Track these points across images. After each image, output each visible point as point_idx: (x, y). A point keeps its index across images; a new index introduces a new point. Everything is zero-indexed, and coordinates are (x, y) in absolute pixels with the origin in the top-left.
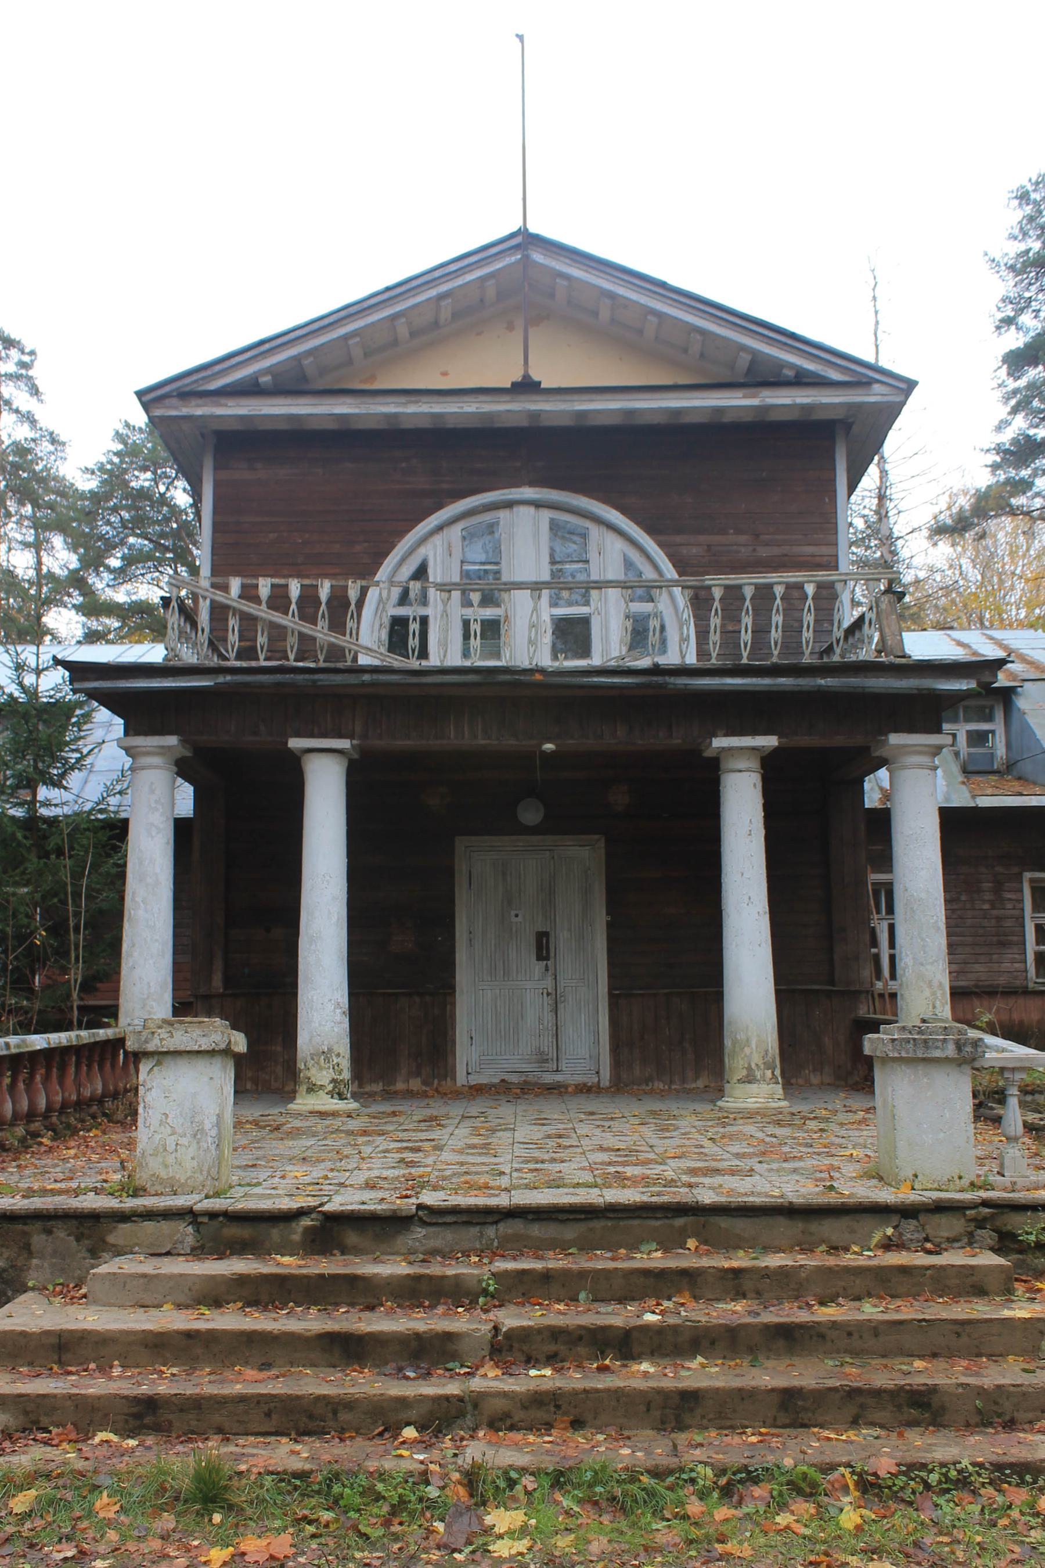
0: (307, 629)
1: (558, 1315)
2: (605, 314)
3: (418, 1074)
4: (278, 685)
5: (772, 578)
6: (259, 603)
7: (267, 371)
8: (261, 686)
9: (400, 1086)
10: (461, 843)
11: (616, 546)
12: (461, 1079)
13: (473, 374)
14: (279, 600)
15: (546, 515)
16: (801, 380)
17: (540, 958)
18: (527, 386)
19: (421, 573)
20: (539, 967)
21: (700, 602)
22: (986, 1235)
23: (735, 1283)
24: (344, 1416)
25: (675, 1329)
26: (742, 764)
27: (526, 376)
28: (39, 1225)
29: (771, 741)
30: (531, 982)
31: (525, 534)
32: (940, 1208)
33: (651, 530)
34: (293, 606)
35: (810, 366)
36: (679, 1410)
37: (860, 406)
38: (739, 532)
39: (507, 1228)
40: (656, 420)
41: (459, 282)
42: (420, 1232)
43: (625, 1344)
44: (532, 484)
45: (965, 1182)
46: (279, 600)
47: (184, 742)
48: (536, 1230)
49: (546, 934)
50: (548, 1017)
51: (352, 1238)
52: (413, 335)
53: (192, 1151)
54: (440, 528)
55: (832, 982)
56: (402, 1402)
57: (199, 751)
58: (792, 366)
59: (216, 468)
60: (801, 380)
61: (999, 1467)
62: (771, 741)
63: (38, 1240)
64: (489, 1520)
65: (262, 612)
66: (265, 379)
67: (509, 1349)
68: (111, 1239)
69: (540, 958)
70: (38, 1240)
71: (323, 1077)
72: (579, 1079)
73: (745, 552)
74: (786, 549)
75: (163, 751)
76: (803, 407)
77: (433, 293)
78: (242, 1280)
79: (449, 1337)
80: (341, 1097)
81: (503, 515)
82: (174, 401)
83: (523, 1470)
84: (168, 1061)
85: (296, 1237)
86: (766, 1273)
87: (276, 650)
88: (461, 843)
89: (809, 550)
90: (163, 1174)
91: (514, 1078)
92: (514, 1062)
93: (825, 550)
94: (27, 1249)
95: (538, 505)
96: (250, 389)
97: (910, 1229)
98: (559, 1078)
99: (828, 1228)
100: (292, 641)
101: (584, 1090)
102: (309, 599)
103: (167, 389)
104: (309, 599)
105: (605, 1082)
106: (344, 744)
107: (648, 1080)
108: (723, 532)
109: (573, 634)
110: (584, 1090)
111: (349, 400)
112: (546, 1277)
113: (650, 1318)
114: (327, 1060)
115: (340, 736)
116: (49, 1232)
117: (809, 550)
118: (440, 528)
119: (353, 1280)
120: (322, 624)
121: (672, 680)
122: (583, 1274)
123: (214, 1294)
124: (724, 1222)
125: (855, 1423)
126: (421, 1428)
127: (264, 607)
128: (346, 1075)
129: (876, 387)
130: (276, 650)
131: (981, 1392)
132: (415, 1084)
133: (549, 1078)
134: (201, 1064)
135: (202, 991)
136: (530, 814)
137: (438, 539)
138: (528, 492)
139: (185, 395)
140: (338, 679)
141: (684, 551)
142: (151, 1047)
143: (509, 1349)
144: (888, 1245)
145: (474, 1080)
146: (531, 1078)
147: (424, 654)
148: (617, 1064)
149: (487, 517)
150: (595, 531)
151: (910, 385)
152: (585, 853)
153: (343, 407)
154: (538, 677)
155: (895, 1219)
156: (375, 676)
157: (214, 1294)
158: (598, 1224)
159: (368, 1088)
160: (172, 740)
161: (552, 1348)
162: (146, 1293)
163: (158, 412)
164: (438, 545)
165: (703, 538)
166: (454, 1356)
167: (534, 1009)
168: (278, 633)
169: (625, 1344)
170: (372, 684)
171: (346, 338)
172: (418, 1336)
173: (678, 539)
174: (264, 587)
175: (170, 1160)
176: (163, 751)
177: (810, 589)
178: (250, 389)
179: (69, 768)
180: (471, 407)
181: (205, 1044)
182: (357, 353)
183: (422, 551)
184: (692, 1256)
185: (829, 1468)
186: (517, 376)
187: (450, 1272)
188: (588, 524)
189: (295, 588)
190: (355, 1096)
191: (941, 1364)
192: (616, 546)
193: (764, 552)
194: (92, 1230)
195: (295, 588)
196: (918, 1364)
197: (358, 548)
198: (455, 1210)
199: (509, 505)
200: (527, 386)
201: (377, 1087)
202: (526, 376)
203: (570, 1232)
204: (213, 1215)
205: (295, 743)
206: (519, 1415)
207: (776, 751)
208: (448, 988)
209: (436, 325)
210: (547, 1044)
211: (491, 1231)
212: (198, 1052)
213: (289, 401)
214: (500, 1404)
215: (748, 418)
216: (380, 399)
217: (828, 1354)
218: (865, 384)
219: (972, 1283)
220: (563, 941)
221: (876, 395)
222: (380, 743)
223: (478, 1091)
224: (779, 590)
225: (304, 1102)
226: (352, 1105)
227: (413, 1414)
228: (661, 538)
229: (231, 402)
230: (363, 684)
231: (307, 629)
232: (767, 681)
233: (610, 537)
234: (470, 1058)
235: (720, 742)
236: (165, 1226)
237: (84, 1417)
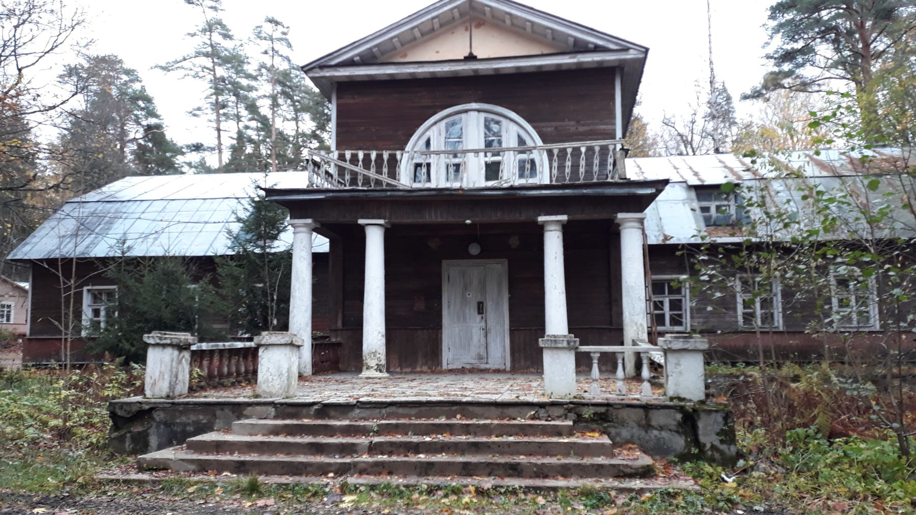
0: (366, 172)
1: (399, 438)
2: (508, 22)
3: (426, 364)
4: (352, 197)
5: (566, 145)
6: (346, 161)
7: (358, 55)
8: (345, 197)
9: (418, 369)
10: (445, 263)
11: (514, 129)
12: (445, 367)
13: (447, 53)
14: (354, 160)
15: (483, 115)
16: (597, 49)
17: (479, 313)
18: (471, 58)
19: (428, 143)
20: (479, 317)
21: (550, 153)
22: (572, 416)
23: (466, 429)
24: (309, 469)
25: (435, 443)
26: (552, 227)
27: (471, 54)
28: (219, 407)
29: (564, 218)
30: (475, 324)
31: (472, 123)
32: (554, 404)
33: (529, 121)
34: (360, 163)
36: (427, 469)
37: (625, 60)
38: (569, 120)
39: (389, 410)
40: (531, 70)
41: (441, 11)
42: (357, 411)
43: (417, 448)
44: (476, 102)
45: (572, 396)
46: (354, 160)
47: (315, 221)
48: (401, 411)
49: (482, 303)
50: (483, 340)
51: (332, 413)
52: (441, 25)
53: (278, 382)
54: (435, 123)
55: (611, 323)
56: (329, 464)
57: (323, 225)
58: (592, 43)
59: (338, 98)
60: (597, 49)
61: (526, 487)
62: (564, 218)
63: (219, 413)
64: (344, 499)
65: (347, 165)
66: (357, 59)
67: (373, 449)
68: (245, 413)
69: (479, 313)
70: (219, 413)
71: (373, 363)
72: (496, 367)
73: (573, 129)
74: (592, 127)
75: (306, 225)
76: (598, 62)
77: (429, 16)
78: (286, 426)
79: (353, 445)
80: (381, 371)
81: (463, 116)
82: (317, 70)
83: (362, 485)
84: (270, 348)
85: (312, 413)
86: (478, 426)
87: (354, 181)
88: (445, 263)
89: (602, 127)
90: (267, 390)
91: (468, 367)
92: (468, 359)
93: (609, 127)
94: (214, 416)
95: (479, 111)
96: (350, 63)
97: (542, 412)
98: (487, 366)
99: (511, 411)
100: (360, 178)
101: (497, 371)
102: (367, 158)
103: (314, 65)
104: (367, 158)
105: (508, 368)
106: (381, 222)
107: (528, 367)
108: (563, 120)
109: (493, 170)
110: (497, 371)
111: (393, 67)
112: (397, 426)
113: (428, 439)
114: (375, 356)
115: (380, 218)
116: (222, 410)
117: (602, 127)
118: (435, 123)
119: (326, 427)
120: (373, 170)
121: (519, 192)
122: (410, 425)
123: (276, 431)
124: (471, 408)
125: (489, 475)
126: (335, 474)
127: (348, 163)
128: (383, 362)
129: (631, 51)
130: (354, 181)
131: (536, 465)
132: (425, 368)
133: (483, 366)
134: (282, 349)
135: (333, 328)
136: (474, 249)
137: (435, 128)
138: (474, 105)
139: (322, 67)
140: (377, 194)
141: (545, 130)
142: (263, 342)
143: (373, 449)
144: (533, 418)
145: (450, 367)
146: (475, 366)
147: (429, 179)
148: (513, 360)
149: (456, 117)
150: (504, 122)
151: (647, 50)
152: (499, 266)
154: (460, 192)
155: (537, 408)
156: (393, 193)
157: (276, 431)
158: (423, 409)
159: (404, 370)
160: (309, 221)
161: (391, 449)
162: (253, 430)
163: (311, 75)
164: (434, 131)
165: (554, 124)
166: (356, 452)
167: (477, 335)
168: (354, 175)
169: (417, 448)
170: (391, 196)
171: (392, 38)
172: (342, 444)
173: (542, 124)
174: (348, 154)
175: (270, 385)
176: (306, 225)
177: (583, 150)
178: (350, 63)
179: (280, 232)
180: (446, 68)
181: (283, 341)
182: (398, 45)
183: (428, 133)
184: (458, 420)
185: (466, 486)
186: (467, 54)
187: (362, 424)
189: (361, 154)
190: (388, 371)
191: (531, 457)
192: (514, 128)
193: (582, 129)
194: (238, 409)
195: (361, 154)
196: (522, 457)
197: (400, 133)
198: (370, 403)
199: (466, 111)
200: (471, 58)
201: (409, 370)
202: (471, 54)
203: (414, 411)
204: (282, 404)
205: (361, 221)
206: (370, 470)
207: (569, 221)
208: (439, 327)
209: (433, 30)
210: (482, 351)
211: (384, 411)
212: (281, 345)
213: (366, 68)
214: (363, 465)
215: (574, 67)
216: (406, 66)
217: (490, 453)
218: (626, 49)
219: (558, 431)
220: (489, 306)
221: (631, 55)
222: (397, 220)
223: (451, 371)
224: (569, 151)
225: (365, 373)
226: (386, 375)
227: (333, 468)
228: (535, 124)
229: (341, 69)
230: (387, 196)
231: (366, 172)
232: (560, 191)
233: (512, 125)
234: (449, 357)
235: (541, 219)
236: (264, 408)
237: (220, 467)
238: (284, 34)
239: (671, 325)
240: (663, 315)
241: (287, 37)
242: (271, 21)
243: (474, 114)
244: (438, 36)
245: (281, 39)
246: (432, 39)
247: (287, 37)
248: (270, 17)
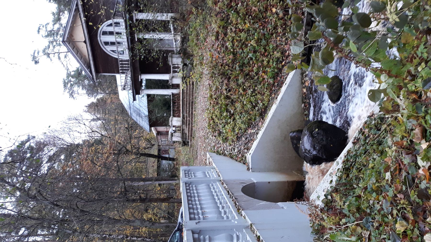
54: (105, 49)
81: (102, 41)
95: (100, 37)
118: (105, 49)
137: (107, 49)
153: (92, 62)
164: (108, 49)
183: (109, 50)
199: (101, 41)
238: (43, 26)
241: (44, 25)
242: (39, 32)
244: (82, 53)
245: (46, 28)
246: (79, 49)
247: (44, 25)
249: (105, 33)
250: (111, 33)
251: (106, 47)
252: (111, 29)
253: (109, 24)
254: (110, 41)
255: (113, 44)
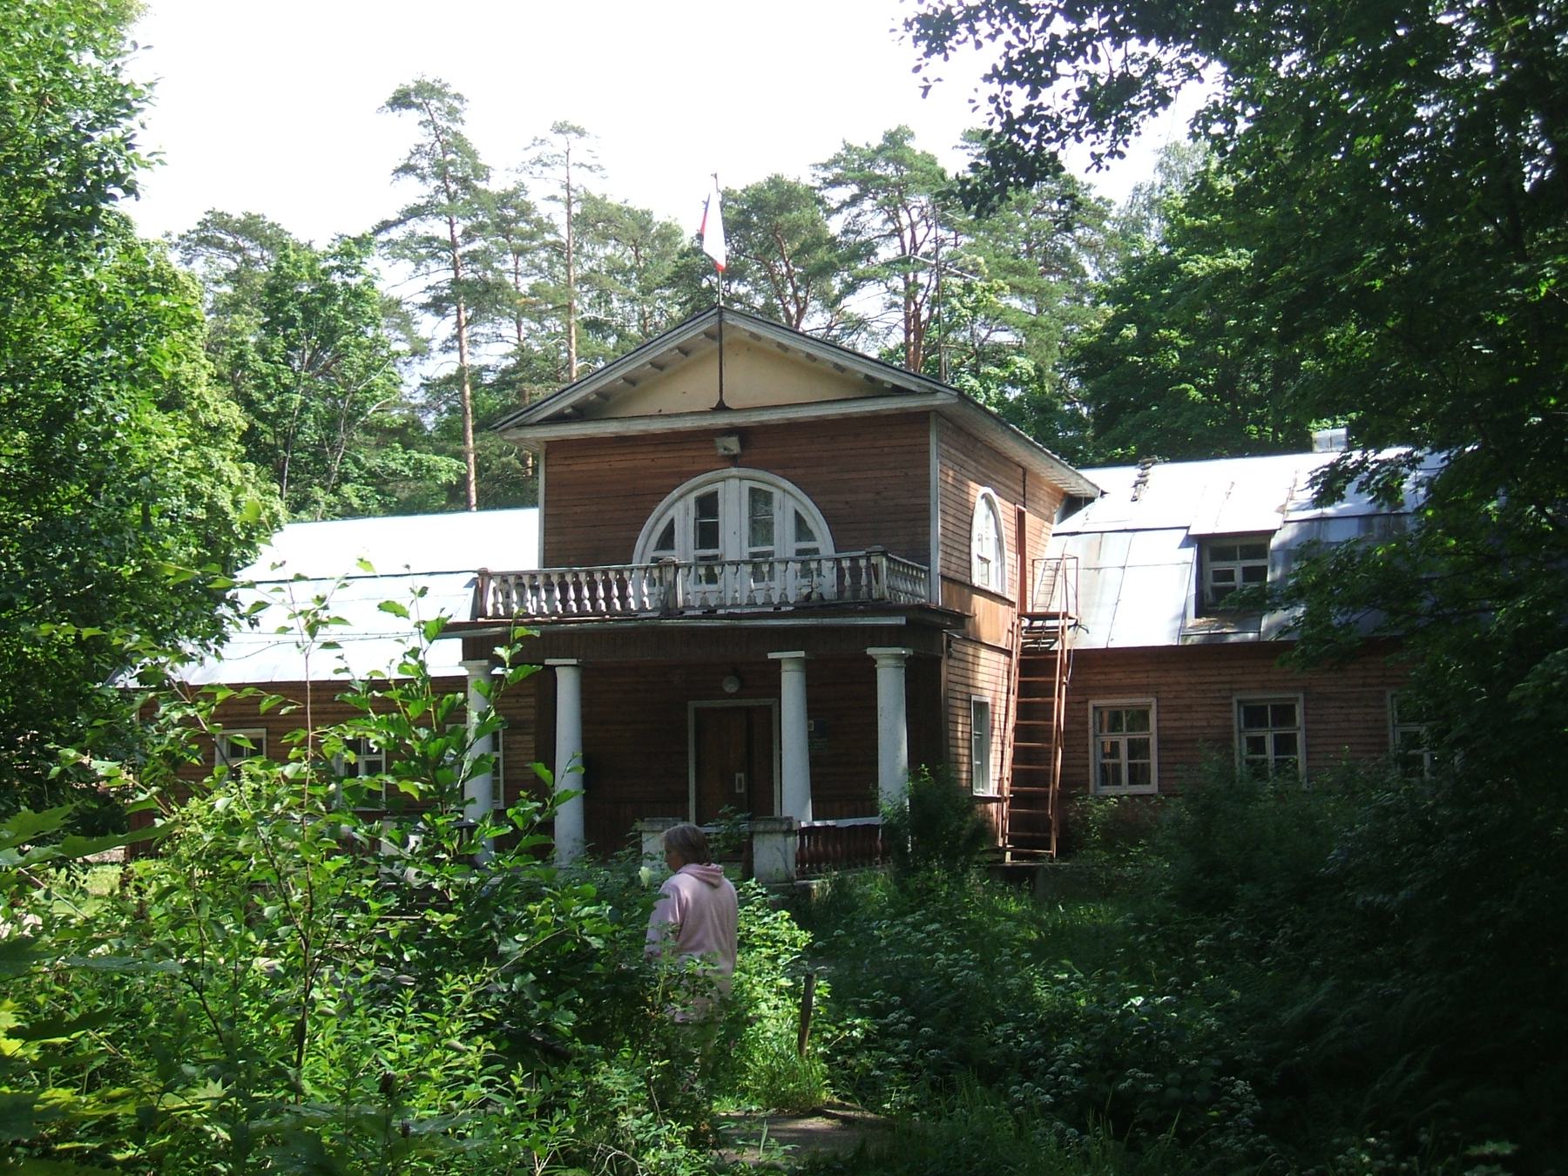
13: (686, 399)
15: (747, 484)
16: (898, 391)
18: (721, 408)
27: (721, 402)
35: (898, 383)
54: (681, 497)
60: (898, 391)
81: (720, 486)
118: (681, 497)
164: (679, 510)
183: (671, 513)
188: (772, 489)
199: (723, 480)
202: (721, 402)
239: (1149, 782)
240: (1117, 767)
243: (734, 483)
248: (560, 120)
249: (759, 499)
250: (761, 528)
251: (691, 499)
252: (784, 528)
253: (811, 524)
254: (720, 520)
255: (708, 535)
